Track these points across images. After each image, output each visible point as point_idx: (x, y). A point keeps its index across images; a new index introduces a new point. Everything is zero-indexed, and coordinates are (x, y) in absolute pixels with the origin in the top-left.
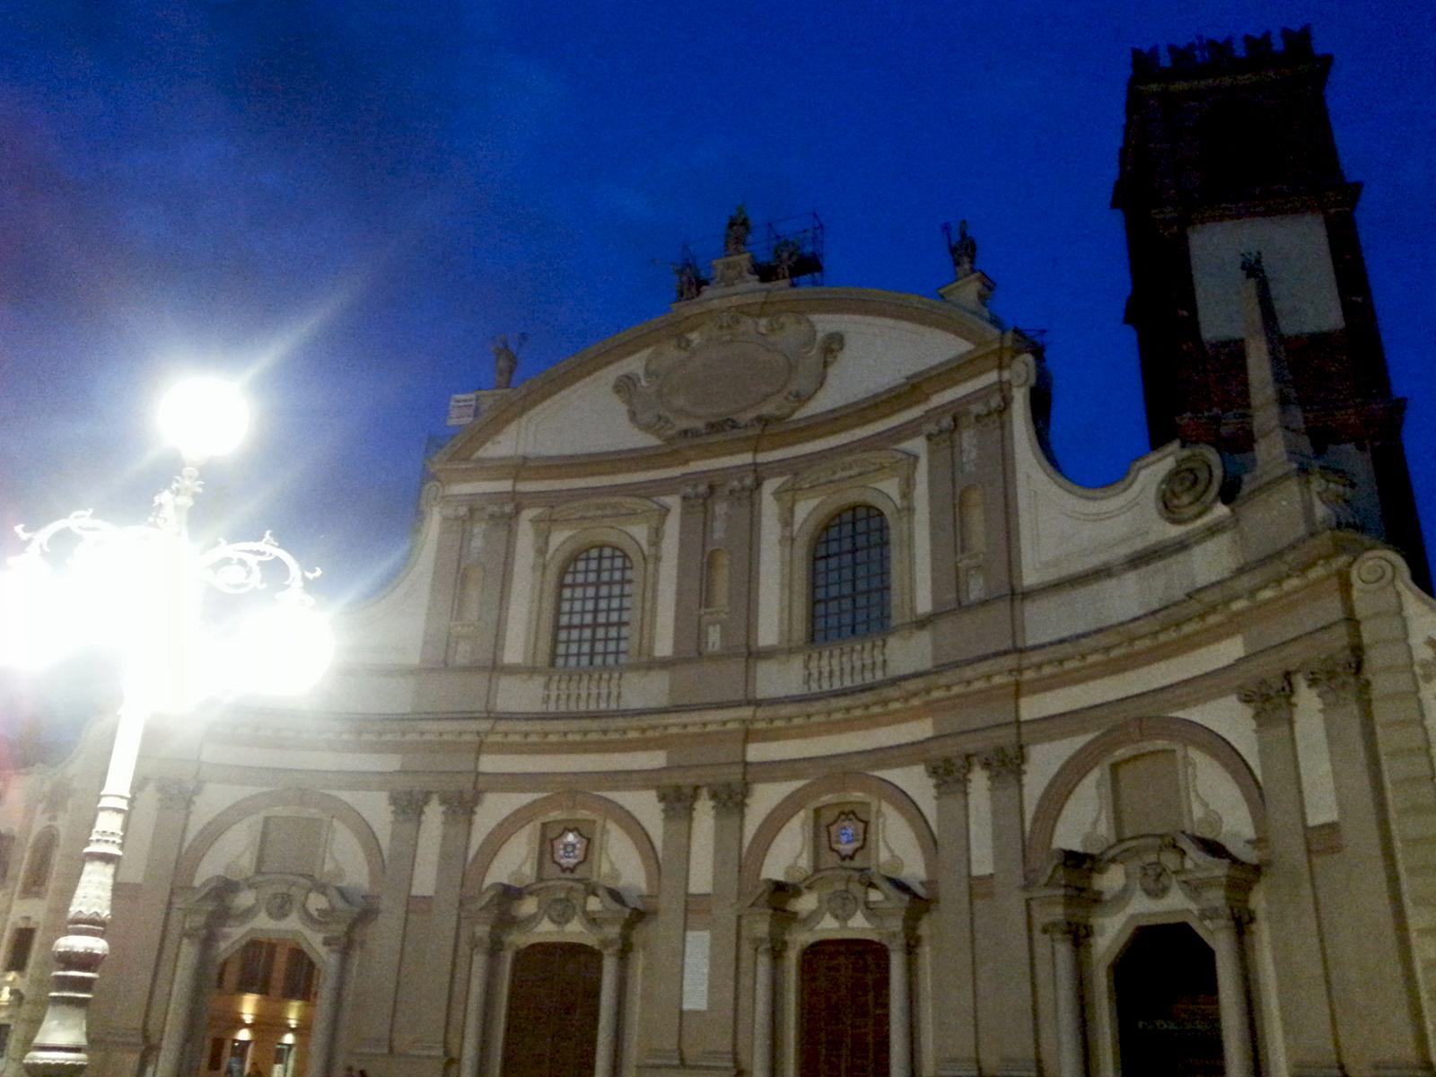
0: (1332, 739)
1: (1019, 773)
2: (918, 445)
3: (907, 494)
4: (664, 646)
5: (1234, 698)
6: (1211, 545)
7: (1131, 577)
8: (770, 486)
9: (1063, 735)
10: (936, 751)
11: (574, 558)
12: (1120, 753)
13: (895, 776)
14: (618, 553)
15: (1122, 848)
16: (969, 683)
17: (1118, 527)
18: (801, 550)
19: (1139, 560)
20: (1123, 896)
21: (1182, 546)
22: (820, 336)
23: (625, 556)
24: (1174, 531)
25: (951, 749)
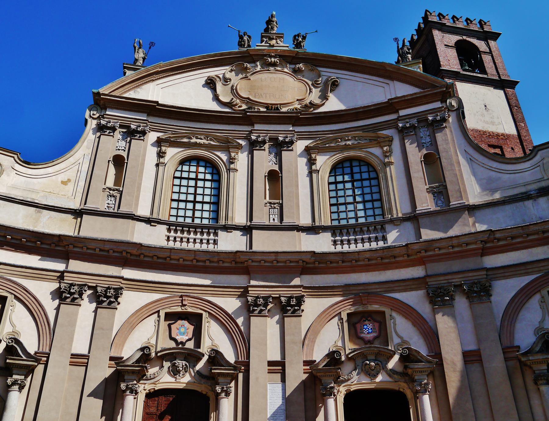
9: (521, 275)
10: (432, 282)
11: (182, 162)
14: (208, 165)
16: (453, 247)
17: (527, 177)
25: (442, 281)
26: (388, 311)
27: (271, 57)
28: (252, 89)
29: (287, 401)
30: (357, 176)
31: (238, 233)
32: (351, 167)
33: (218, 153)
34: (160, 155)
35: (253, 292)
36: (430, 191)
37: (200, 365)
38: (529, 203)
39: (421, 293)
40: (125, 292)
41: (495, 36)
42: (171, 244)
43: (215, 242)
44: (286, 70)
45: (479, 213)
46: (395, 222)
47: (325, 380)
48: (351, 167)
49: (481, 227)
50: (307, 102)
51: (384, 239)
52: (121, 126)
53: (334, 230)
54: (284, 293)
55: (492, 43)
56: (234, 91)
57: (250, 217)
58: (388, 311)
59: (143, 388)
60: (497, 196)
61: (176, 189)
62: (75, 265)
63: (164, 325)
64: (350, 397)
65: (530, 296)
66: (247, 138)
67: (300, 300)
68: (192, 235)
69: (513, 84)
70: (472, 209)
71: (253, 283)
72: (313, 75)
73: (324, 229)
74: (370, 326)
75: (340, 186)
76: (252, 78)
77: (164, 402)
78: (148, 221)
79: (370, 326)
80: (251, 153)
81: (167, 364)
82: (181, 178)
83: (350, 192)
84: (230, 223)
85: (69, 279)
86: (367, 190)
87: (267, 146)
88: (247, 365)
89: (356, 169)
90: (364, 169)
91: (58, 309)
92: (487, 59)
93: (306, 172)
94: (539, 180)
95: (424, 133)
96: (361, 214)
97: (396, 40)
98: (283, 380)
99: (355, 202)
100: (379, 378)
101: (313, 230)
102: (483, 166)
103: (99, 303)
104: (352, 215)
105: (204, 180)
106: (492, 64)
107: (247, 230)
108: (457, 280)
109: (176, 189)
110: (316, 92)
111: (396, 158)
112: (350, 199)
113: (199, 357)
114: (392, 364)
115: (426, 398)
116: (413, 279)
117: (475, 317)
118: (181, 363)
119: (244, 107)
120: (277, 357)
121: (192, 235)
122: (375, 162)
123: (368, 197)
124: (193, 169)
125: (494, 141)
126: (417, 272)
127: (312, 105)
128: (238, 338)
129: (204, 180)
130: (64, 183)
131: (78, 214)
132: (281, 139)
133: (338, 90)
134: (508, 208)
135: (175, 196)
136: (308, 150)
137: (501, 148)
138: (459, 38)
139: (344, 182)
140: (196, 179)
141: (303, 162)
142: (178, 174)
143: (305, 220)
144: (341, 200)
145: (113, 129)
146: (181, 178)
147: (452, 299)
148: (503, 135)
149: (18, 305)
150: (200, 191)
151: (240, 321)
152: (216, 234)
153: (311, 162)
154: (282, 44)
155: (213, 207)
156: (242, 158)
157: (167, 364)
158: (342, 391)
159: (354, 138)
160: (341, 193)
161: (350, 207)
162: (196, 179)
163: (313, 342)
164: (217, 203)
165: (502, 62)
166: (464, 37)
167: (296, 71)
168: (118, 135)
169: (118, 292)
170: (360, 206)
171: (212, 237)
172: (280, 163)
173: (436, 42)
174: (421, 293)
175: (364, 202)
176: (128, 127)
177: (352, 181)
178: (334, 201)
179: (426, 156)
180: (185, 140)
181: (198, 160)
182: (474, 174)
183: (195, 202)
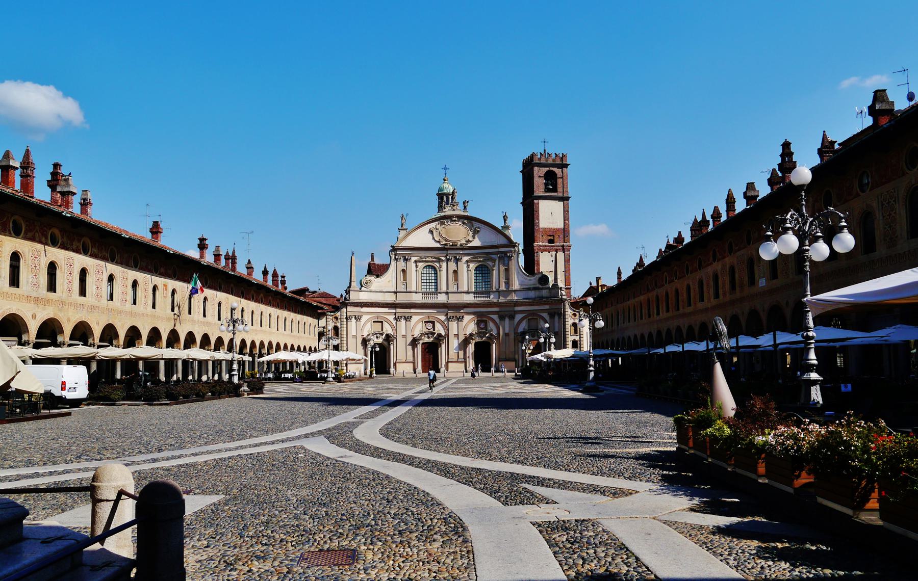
1: (514, 318)
4: (444, 289)
5: (547, 314)
6: (546, 290)
7: (533, 291)
10: (500, 313)
11: (424, 268)
12: (530, 317)
17: (532, 282)
19: (535, 289)
21: (542, 289)
24: (540, 286)
25: (502, 313)
26: (488, 320)
27: (454, 218)
28: (447, 233)
29: (459, 345)
30: (484, 272)
31: (444, 294)
32: (482, 268)
33: (436, 263)
34: (417, 266)
35: (449, 315)
36: (505, 282)
37: (435, 336)
38: (530, 292)
39: (497, 315)
41: (566, 166)
43: (437, 298)
44: (460, 223)
45: (517, 292)
46: (493, 292)
47: (469, 340)
48: (482, 268)
49: (516, 298)
50: (467, 239)
51: (489, 297)
52: (403, 257)
53: (474, 293)
54: (458, 315)
55: (565, 169)
56: (440, 234)
58: (488, 320)
59: (421, 342)
60: (522, 287)
61: (423, 278)
62: (399, 310)
63: (424, 324)
64: (476, 344)
65: (524, 320)
66: (446, 256)
67: (463, 317)
68: (430, 296)
69: (568, 198)
70: (515, 291)
71: (449, 312)
72: (470, 225)
73: (471, 292)
74: (483, 324)
75: (478, 275)
76: (447, 227)
77: (427, 345)
78: (416, 293)
79: (483, 324)
80: (447, 263)
81: (426, 336)
82: (424, 274)
83: (481, 278)
84: (441, 291)
86: (486, 278)
87: (453, 259)
88: (448, 335)
89: (483, 269)
90: (486, 269)
91: (396, 323)
92: (560, 181)
93: (466, 270)
94: (534, 284)
95: (506, 259)
96: (483, 286)
97: (503, 212)
98: (458, 339)
99: (482, 282)
100: (484, 339)
101: (468, 293)
102: (521, 275)
103: (406, 320)
104: (481, 286)
105: (432, 274)
106: (562, 185)
107: (447, 293)
108: (506, 313)
109: (423, 278)
110: (471, 233)
111: (496, 268)
112: (481, 281)
113: (435, 333)
114: (487, 336)
115: (494, 345)
116: (496, 311)
117: (510, 324)
118: (430, 335)
119: (444, 242)
120: (457, 333)
121: (430, 296)
122: (490, 268)
123: (486, 280)
124: (428, 270)
125: (551, 233)
126: (496, 309)
127: (469, 241)
128: (445, 327)
129: (432, 274)
130: (389, 282)
131: (395, 293)
132: (458, 257)
133: (479, 233)
134: (524, 292)
135: (423, 281)
136: (467, 262)
137: (554, 236)
138: (547, 169)
139: (479, 274)
140: (429, 274)
141: (465, 265)
142: (423, 273)
143: (465, 289)
144: (478, 281)
145: (400, 259)
146: (424, 274)
147: (505, 318)
148: (556, 229)
149: (386, 323)
150: (430, 278)
151: (446, 323)
152: (437, 295)
153: (468, 266)
154: (458, 208)
155: (435, 284)
156: (444, 265)
157: (426, 336)
158: (473, 342)
159: (483, 257)
160: (478, 278)
161: (481, 284)
162: (429, 274)
163: (467, 328)
164: (437, 283)
165: (567, 183)
166: (551, 168)
167: (464, 223)
168: (402, 260)
169: (411, 317)
170: (483, 284)
171: (436, 296)
172: (457, 267)
173: (534, 175)
174: (497, 315)
175: (485, 282)
176: (405, 257)
177: (482, 274)
178: (475, 281)
179: (505, 269)
180: (424, 259)
181: (429, 266)
182: (518, 280)
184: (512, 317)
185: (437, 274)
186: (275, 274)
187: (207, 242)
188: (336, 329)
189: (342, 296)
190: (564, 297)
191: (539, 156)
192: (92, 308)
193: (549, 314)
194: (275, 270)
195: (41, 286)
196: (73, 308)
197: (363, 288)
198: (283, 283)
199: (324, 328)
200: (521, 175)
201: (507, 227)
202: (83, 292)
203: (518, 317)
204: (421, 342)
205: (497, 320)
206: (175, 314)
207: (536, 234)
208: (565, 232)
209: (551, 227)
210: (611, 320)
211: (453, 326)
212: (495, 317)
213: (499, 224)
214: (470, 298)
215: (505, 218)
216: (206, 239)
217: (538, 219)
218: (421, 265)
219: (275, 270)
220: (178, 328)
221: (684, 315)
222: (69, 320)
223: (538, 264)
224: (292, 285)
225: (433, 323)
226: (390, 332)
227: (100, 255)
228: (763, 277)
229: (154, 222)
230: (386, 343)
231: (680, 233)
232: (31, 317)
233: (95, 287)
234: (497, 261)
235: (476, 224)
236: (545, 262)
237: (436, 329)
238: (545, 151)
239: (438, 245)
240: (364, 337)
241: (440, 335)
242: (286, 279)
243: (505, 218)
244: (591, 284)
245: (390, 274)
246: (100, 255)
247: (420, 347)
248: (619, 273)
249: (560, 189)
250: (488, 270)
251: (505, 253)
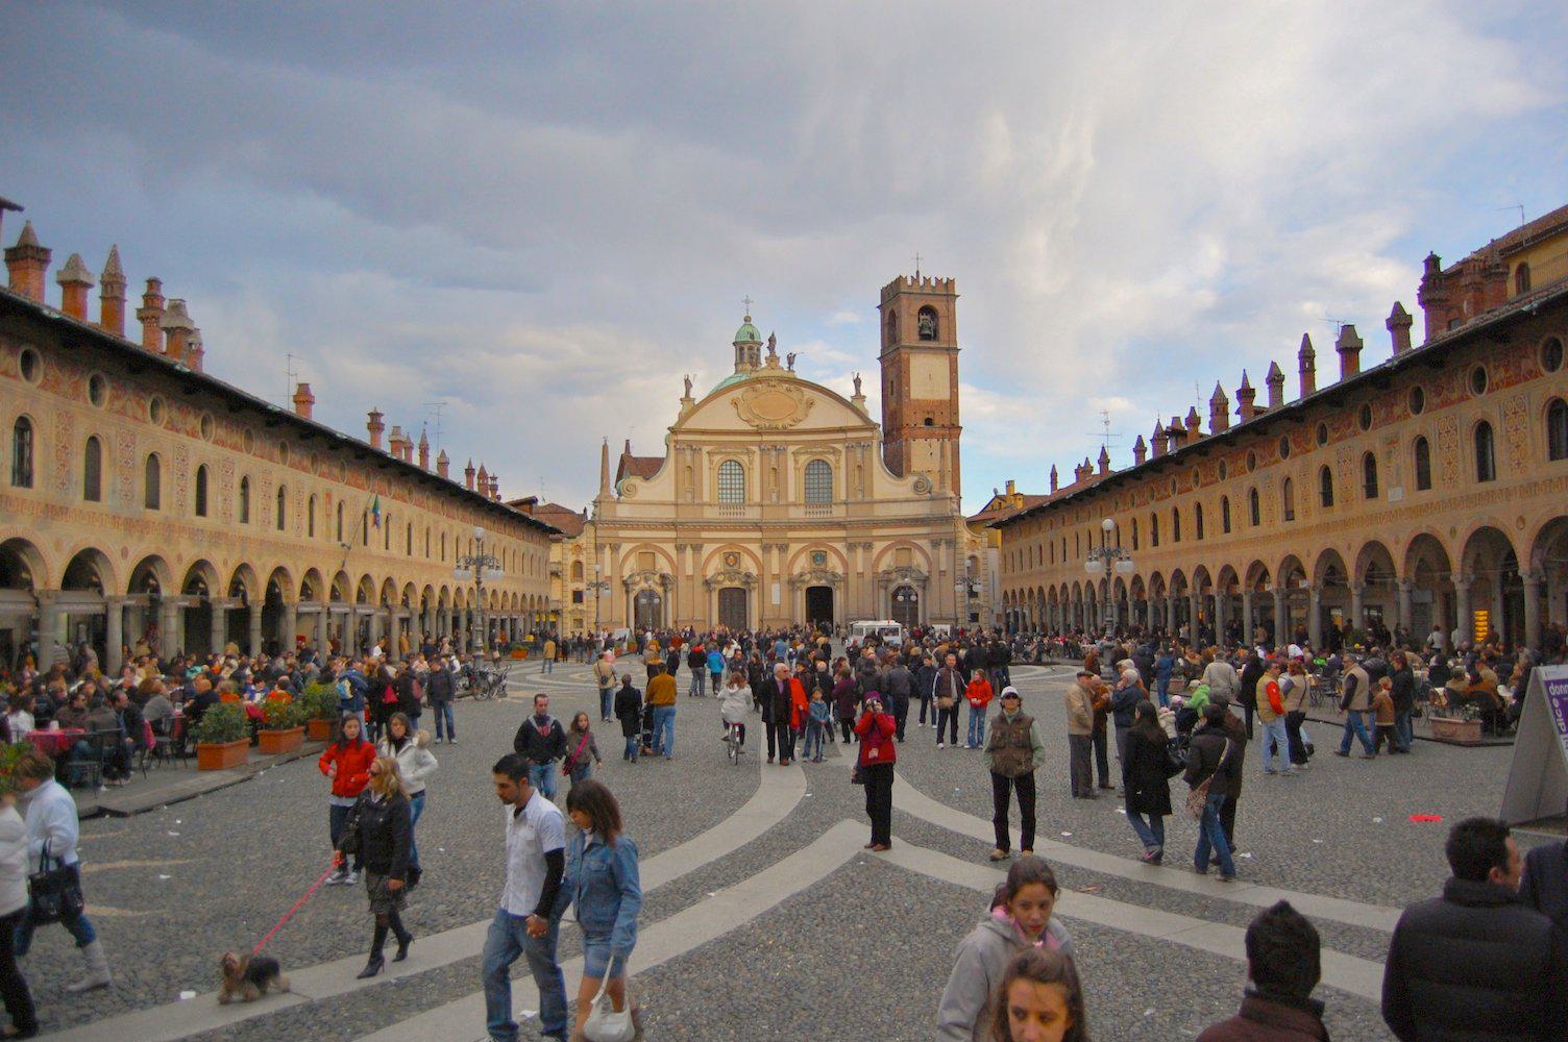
0: (948, 555)
2: (838, 446)
3: (837, 461)
4: (757, 498)
8: (791, 449)
10: (850, 541)
13: (835, 545)
15: (898, 570)
18: (802, 471)
19: (907, 501)
20: (896, 580)
22: (806, 397)
23: (740, 465)
40: (705, 545)
42: (722, 517)
57: (762, 499)
78: (710, 505)
85: (679, 542)
89: (821, 467)
90: (825, 467)
92: (943, 323)
108: (858, 540)
112: (816, 486)
126: (842, 533)
183: (731, 489)
184: (868, 547)
185: (743, 474)
186: (483, 475)
187: (382, 420)
188: (578, 564)
189: (585, 510)
190: (955, 514)
191: (909, 282)
192: (217, 537)
193: (932, 542)
194: (482, 468)
195: (136, 498)
196: (187, 536)
197: (622, 498)
198: (494, 488)
199: (559, 563)
200: (878, 313)
201: (859, 396)
202: (201, 510)
203: (879, 546)
204: (719, 587)
205: (844, 551)
206: (343, 545)
207: (904, 409)
208: (953, 404)
209: (928, 398)
210: (1049, 552)
211: (775, 561)
212: (840, 546)
213: (847, 390)
214: (797, 514)
215: (857, 382)
216: (381, 415)
217: (908, 384)
218: (717, 458)
219: (482, 468)
220: (349, 570)
221: (1212, 548)
222: (180, 558)
223: (909, 460)
224: (508, 495)
225: (737, 560)
226: (667, 570)
227: (229, 442)
228: (1397, 485)
229: (300, 385)
230: (659, 590)
231: (1193, 409)
232: (120, 553)
233: (220, 499)
234: (843, 454)
235: (808, 393)
236: (923, 453)
237: (743, 565)
238: (918, 272)
239: (747, 427)
240: (625, 578)
241: (748, 576)
242: (498, 482)
243: (857, 382)
244: (995, 491)
245: (667, 474)
246: (229, 442)
247: (715, 597)
248: (1054, 476)
249: (943, 333)
250: (829, 468)
251: (858, 441)
